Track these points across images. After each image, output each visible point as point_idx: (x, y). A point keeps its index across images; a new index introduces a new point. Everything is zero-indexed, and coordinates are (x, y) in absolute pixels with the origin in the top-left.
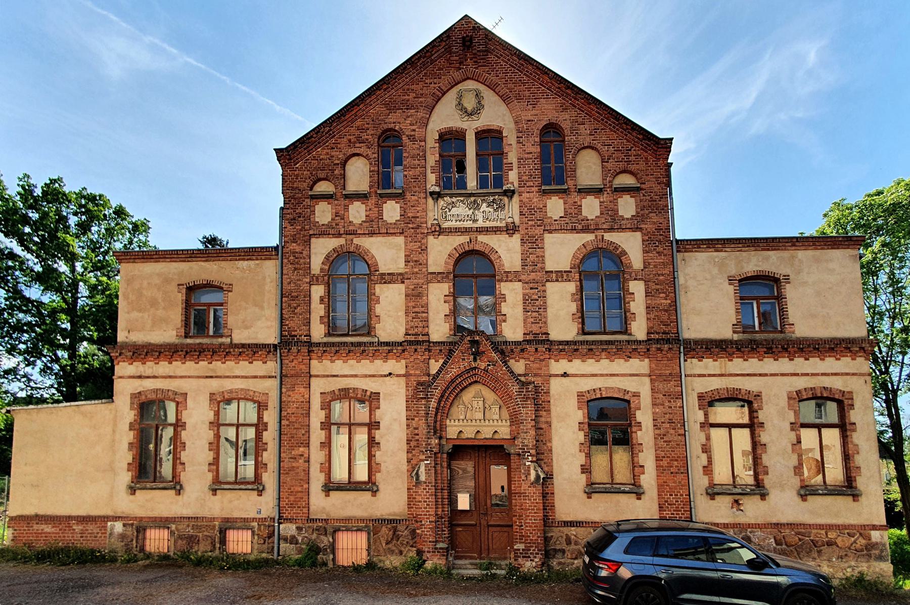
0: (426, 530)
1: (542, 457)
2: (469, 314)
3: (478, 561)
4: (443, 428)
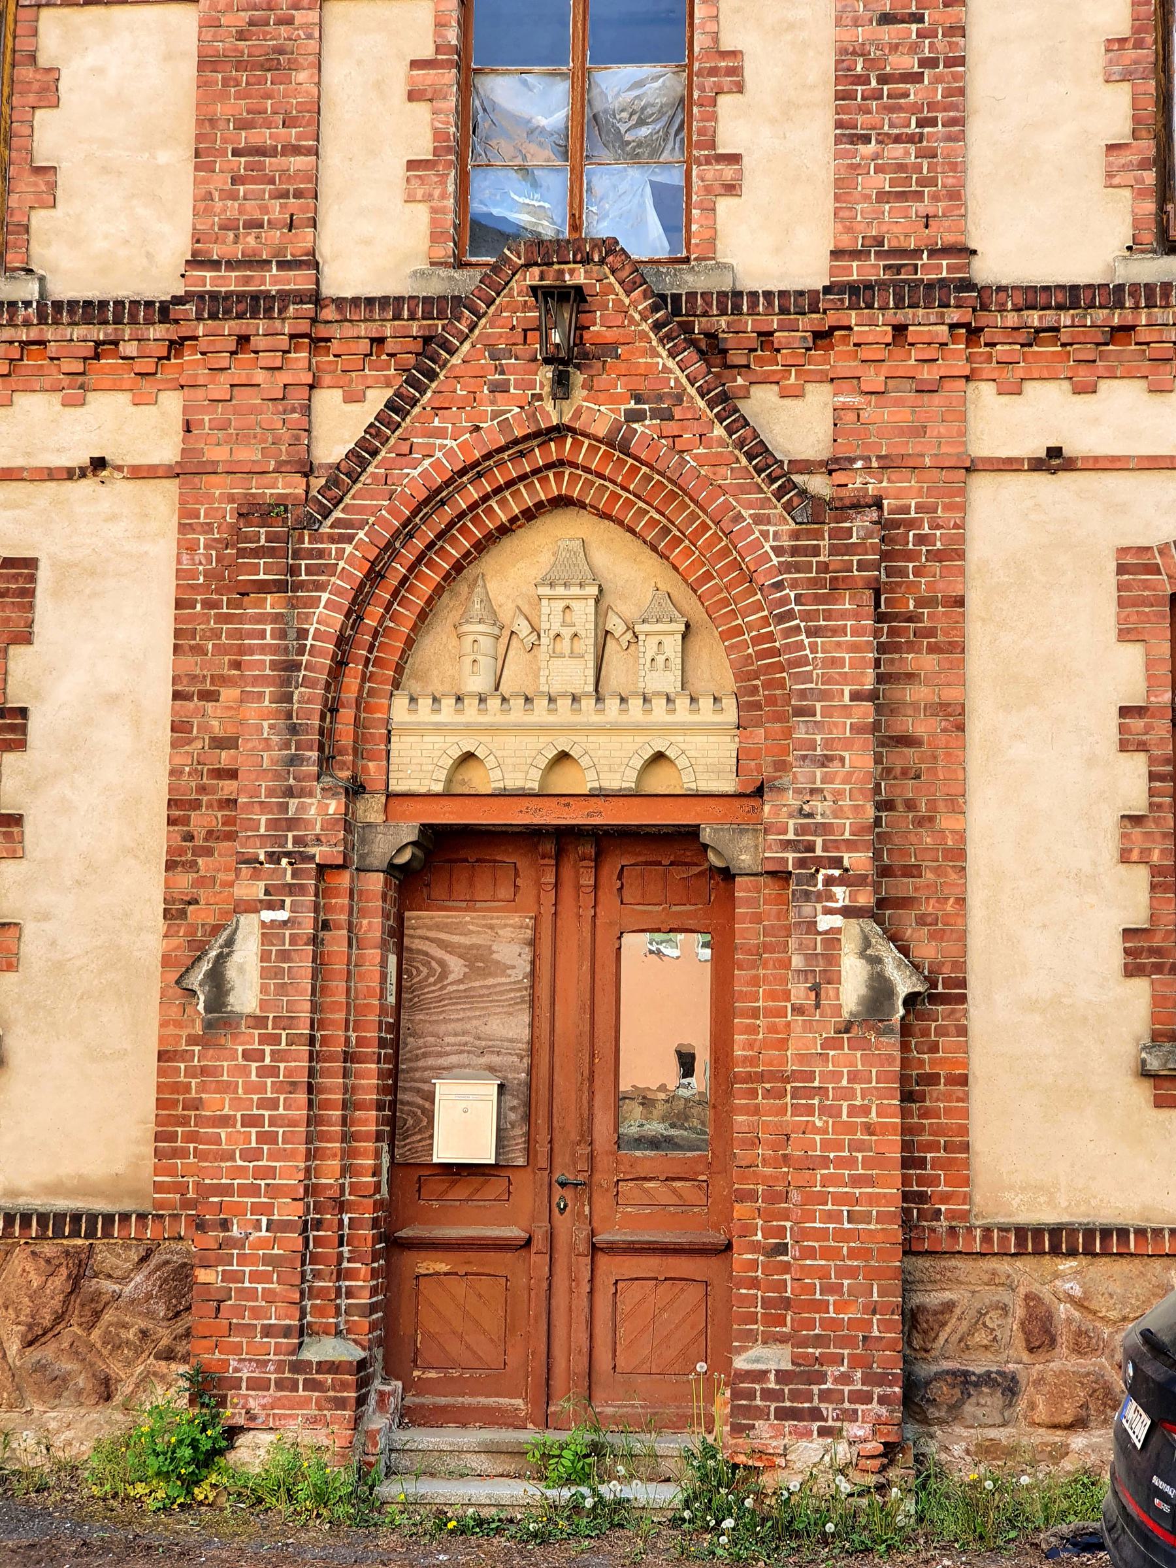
0: (253, 1272)
1: (904, 887)
2: (541, 155)
3: (529, 1436)
4: (372, 739)
